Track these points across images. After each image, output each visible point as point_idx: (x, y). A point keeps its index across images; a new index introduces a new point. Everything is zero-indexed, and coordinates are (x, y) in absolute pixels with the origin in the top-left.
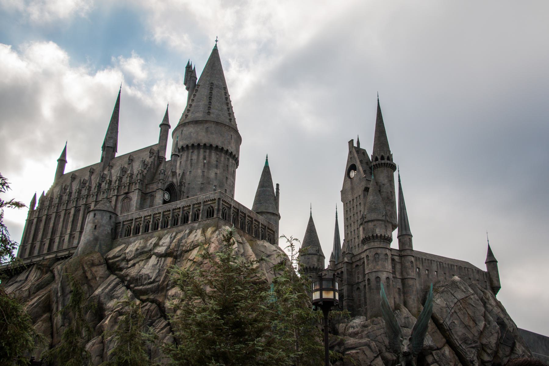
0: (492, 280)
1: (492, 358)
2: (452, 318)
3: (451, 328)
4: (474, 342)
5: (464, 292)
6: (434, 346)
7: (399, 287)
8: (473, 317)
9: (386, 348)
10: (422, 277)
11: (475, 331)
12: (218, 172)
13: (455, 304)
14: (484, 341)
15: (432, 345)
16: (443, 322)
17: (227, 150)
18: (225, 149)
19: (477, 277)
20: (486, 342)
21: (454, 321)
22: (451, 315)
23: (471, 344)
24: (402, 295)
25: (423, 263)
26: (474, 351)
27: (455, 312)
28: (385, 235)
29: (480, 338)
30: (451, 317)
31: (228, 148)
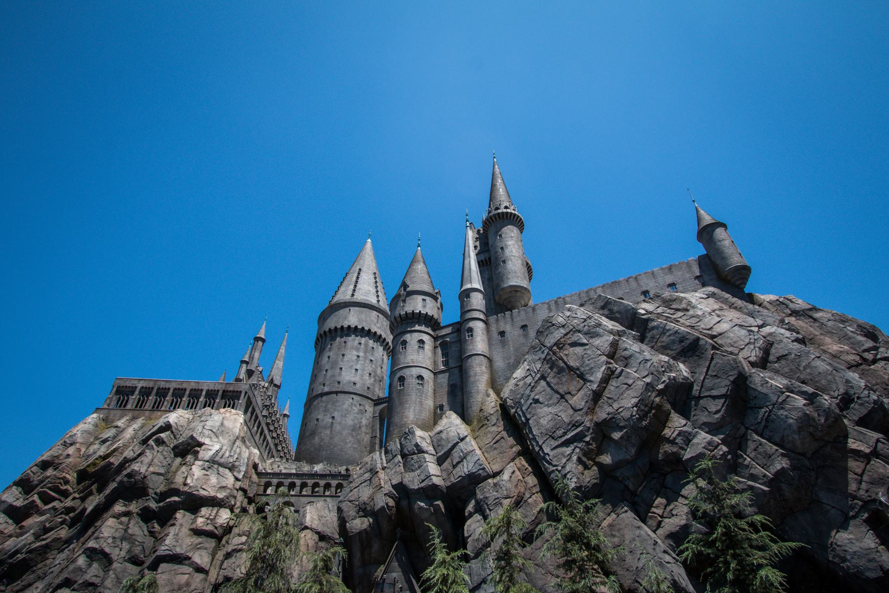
0: (717, 265)
1: (633, 451)
2: (533, 395)
3: (528, 416)
4: (574, 425)
5: (563, 326)
6: (481, 472)
7: (454, 382)
8: (578, 369)
9: (360, 508)
10: (511, 343)
11: (579, 399)
12: (331, 354)
13: (544, 359)
14: (602, 414)
15: (474, 471)
16: (516, 412)
17: (342, 327)
18: (339, 327)
19: (670, 279)
20: (608, 414)
21: (537, 397)
22: (532, 388)
23: (565, 434)
24: (459, 394)
25: (512, 320)
26: (568, 450)
27: (543, 377)
28: (400, 314)
29: (591, 410)
30: (531, 391)
31: (343, 324)
